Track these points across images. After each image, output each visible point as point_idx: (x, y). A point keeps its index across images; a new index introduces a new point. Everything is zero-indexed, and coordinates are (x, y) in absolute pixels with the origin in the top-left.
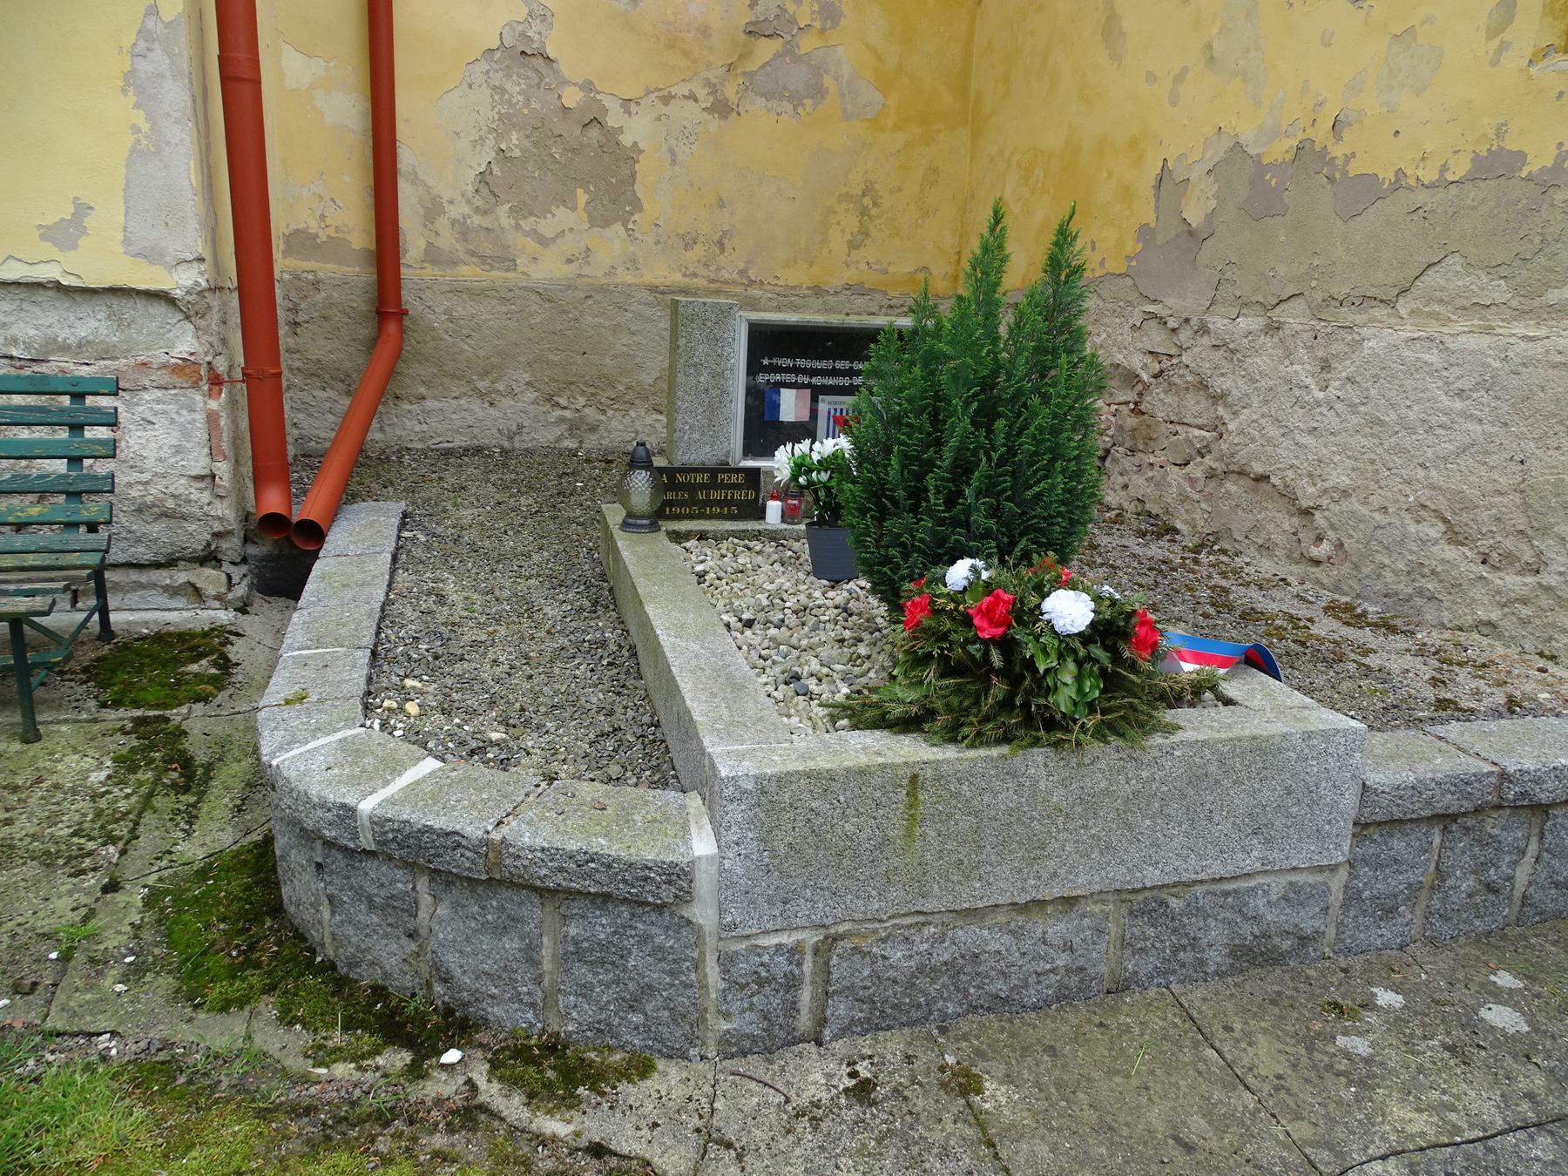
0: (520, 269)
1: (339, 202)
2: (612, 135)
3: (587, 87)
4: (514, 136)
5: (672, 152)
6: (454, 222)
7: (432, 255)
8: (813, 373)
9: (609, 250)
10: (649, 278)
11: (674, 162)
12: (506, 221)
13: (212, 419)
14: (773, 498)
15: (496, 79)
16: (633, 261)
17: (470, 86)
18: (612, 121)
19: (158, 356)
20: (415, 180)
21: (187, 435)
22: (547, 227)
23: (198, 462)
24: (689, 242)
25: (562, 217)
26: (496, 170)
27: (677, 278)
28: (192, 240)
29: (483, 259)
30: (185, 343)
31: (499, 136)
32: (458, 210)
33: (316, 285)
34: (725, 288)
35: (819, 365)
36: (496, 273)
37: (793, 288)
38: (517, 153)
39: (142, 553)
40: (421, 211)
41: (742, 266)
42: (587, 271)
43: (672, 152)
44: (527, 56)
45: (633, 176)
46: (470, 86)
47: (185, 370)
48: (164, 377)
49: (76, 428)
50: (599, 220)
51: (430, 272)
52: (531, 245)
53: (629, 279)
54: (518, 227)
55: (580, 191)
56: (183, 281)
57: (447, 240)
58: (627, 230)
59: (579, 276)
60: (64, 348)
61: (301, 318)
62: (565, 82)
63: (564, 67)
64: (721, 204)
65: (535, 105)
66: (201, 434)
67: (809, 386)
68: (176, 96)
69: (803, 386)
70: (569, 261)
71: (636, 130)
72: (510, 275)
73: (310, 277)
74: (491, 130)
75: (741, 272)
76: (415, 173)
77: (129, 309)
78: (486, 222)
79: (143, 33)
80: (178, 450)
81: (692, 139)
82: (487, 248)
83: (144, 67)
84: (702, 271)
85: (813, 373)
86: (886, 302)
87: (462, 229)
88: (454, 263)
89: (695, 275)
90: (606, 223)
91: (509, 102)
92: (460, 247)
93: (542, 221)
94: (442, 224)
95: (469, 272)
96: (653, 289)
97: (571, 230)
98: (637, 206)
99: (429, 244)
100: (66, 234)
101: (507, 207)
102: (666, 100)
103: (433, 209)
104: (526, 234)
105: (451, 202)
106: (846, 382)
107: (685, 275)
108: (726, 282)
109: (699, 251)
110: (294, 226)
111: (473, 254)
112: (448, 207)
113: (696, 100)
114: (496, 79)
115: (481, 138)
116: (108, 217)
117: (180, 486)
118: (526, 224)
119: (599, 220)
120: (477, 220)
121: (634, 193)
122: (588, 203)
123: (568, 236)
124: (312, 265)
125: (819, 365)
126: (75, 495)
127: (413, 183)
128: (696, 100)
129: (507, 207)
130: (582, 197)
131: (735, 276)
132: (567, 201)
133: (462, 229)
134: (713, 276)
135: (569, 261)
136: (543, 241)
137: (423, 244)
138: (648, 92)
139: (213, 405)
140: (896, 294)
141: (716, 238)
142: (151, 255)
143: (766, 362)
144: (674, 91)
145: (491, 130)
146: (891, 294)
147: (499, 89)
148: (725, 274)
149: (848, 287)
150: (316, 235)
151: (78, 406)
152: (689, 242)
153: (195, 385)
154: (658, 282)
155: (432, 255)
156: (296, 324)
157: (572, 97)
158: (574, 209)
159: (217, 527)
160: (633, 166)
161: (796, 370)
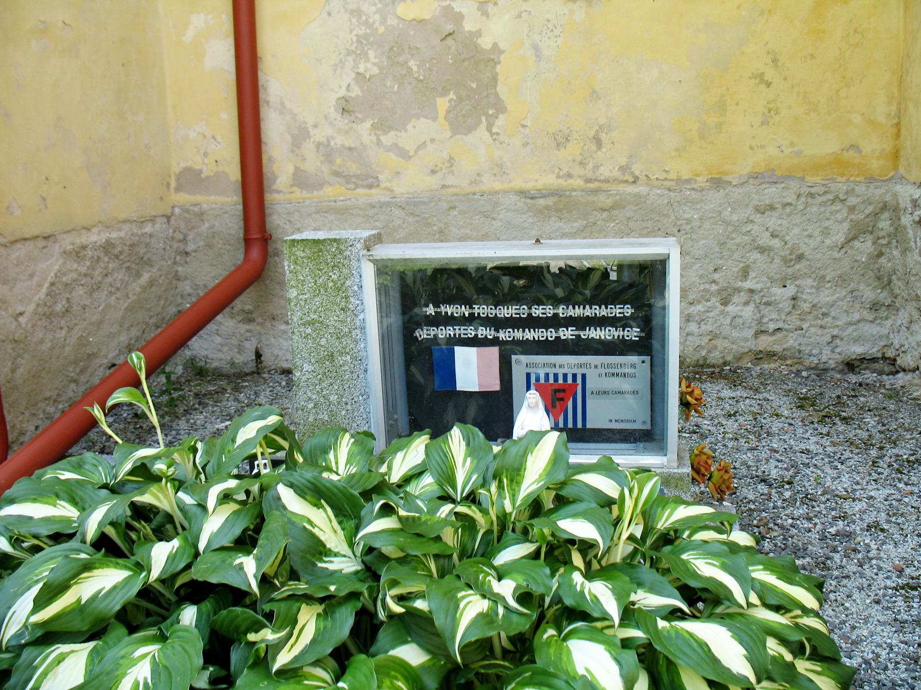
0: (383, 185)
1: (219, 138)
5: (536, 48)
6: (318, 145)
8: (497, 323)
9: (476, 157)
16: (501, 166)
17: (329, 14)
20: (283, 110)
22: (408, 138)
24: (561, 141)
25: (421, 128)
27: (550, 180)
29: (347, 179)
32: (318, 135)
33: (201, 215)
34: (605, 186)
35: (507, 312)
37: (688, 181)
40: (289, 137)
41: (623, 161)
43: (536, 48)
45: (495, 79)
46: (329, 14)
50: (461, 124)
53: (497, 185)
54: (379, 143)
57: (312, 163)
58: (492, 134)
59: (444, 187)
61: (191, 247)
64: (594, 95)
67: (495, 342)
69: (495, 342)
70: (433, 172)
71: (495, 31)
72: (373, 191)
73: (196, 209)
75: (622, 169)
76: (282, 104)
78: (349, 143)
81: (557, 32)
82: (353, 168)
84: (577, 170)
85: (497, 323)
86: (805, 190)
88: (320, 185)
89: (570, 176)
90: (470, 129)
91: (366, 23)
92: (325, 168)
93: (403, 134)
94: (308, 148)
95: (332, 191)
96: (522, 193)
97: (432, 140)
98: (500, 108)
99: (297, 169)
101: (368, 124)
103: (300, 136)
104: (388, 149)
105: (315, 126)
106: (550, 334)
107: (558, 177)
108: (606, 181)
109: (573, 150)
111: (337, 174)
112: (312, 132)
115: (341, 61)
118: (388, 139)
119: (461, 124)
121: (497, 95)
122: (448, 112)
123: (430, 147)
124: (198, 198)
125: (507, 312)
127: (281, 113)
129: (368, 124)
130: (443, 104)
131: (616, 173)
133: (327, 151)
134: (590, 175)
135: (433, 172)
136: (403, 154)
137: (291, 169)
140: (818, 179)
141: (592, 133)
143: (431, 310)
146: (811, 180)
148: (605, 172)
149: (755, 176)
150: (201, 171)
152: (561, 141)
154: (529, 186)
155: (301, 180)
156: (187, 253)
158: (435, 119)
160: (494, 68)
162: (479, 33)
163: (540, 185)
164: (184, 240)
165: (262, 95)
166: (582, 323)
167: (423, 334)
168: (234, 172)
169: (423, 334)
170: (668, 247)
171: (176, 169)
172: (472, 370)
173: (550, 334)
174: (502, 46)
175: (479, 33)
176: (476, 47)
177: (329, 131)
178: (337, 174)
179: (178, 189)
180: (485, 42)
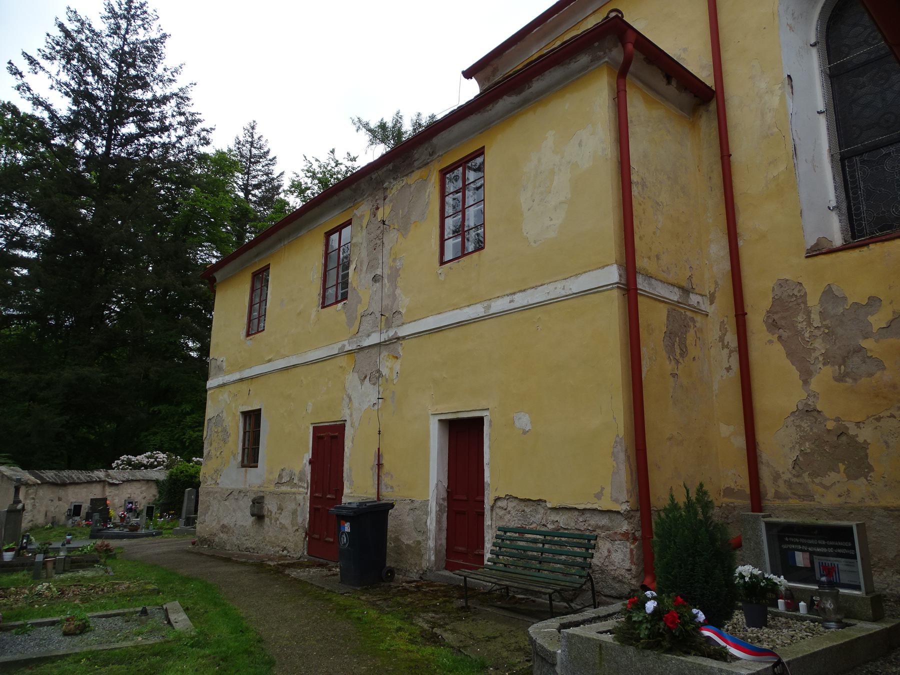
2: (853, 438)
3: (838, 420)
4: (807, 444)
5: (886, 443)
6: (785, 481)
7: (778, 495)
9: (859, 490)
10: (883, 503)
11: (888, 447)
12: (807, 479)
13: (631, 550)
14: (781, 598)
15: (798, 422)
16: (874, 495)
18: (852, 432)
19: (619, 531)
21: (625, 556)
22: (827, 481)
23: (627, 565)
25: (833, 476)
26: (801, 459)
28: (624, 496)
29: (799, 497)
30: (625, 527)
31: (801, 445)
33: (734, 508)
35: (810, 542)
36: (805, 502)
38: (809, 451)
39: (613, 593)
42: (849, 500)
43: (886, 443)
44: (808, 411)
45: (867, 455)
47: (625, 535)
48: (620, 537)
49: (587, 549)
50: (852, 477)
51: (778, 502)
52: (821, 490)
53: (873, 504)
54: (813, 482)
55: (840, 464)
56: (623, 508)
57: (783, 489)
60: (599, 527)
62: (826, 419)
63: (827, 414)
65: (815, 430)
66: (628, 556)
68: (622, 456)
69: (807, 551)
70: (840, 496)
71: (865, 434)
72: (812, 503)
74: (797, 443)
77: (614, 516)
78: (799, 480)
79: (616, 442)
80: (623, 560)
83: (616, 450)
87: (788, 483)
88: (787, 499)
90: (856, 478)
94: (781, 482)
95: (794, 502)
96: (886, 509)
98: (871, 469)
100: (599, 496)
102: (878, 419)
103: (776, 477)
104: (817, 484)
106: (825, 550)
110: (726, 486)
111: (794, 494)
112: (782, 475)
113: (895, 417)
114: (798, 422)
116: (608, 491)
117: (623, 572)
118: (817, 480)
119: (852, 477)
120: (795, 480)
125: (810, 542)
126: (583, 568)
128: (895, 417)
130: (842, 467)
132: (836, 470)
133: (788, 483)
136: (827, 488)
137: (773, 491)
138: (868, 418)
139: (632, 547)
142: (616, 501)
144: (881, 415)
145: (797, 443)
147: (800, 426)
151: (588, 541)
153: (627, 540)
154: (889, 505)
155: (778, 495)
157: (830, 425)
158: (839, 472)
159: (633, 588)
161: (802, 544)
162: (857, 436)
163: (895, 505)
164: (727, 518)
165: (759, 459)
166: (835, 547)
167: (784, 547)
168: (748, 491)
169: (784, 547)
170: (853, 524)
171: (723, 488)
172: (801, 559)
173: (825, 550)
174: (869, 441)
175: (857, 436)
176: (856, 442)
177: (790, 476)
178: (794, 494)
179: (724, 496)
180: (861, 439)
